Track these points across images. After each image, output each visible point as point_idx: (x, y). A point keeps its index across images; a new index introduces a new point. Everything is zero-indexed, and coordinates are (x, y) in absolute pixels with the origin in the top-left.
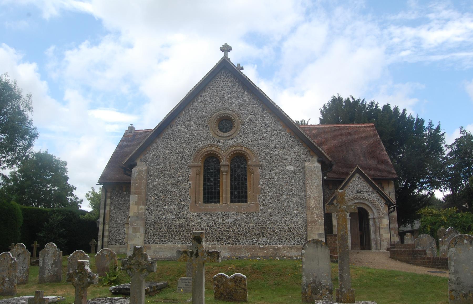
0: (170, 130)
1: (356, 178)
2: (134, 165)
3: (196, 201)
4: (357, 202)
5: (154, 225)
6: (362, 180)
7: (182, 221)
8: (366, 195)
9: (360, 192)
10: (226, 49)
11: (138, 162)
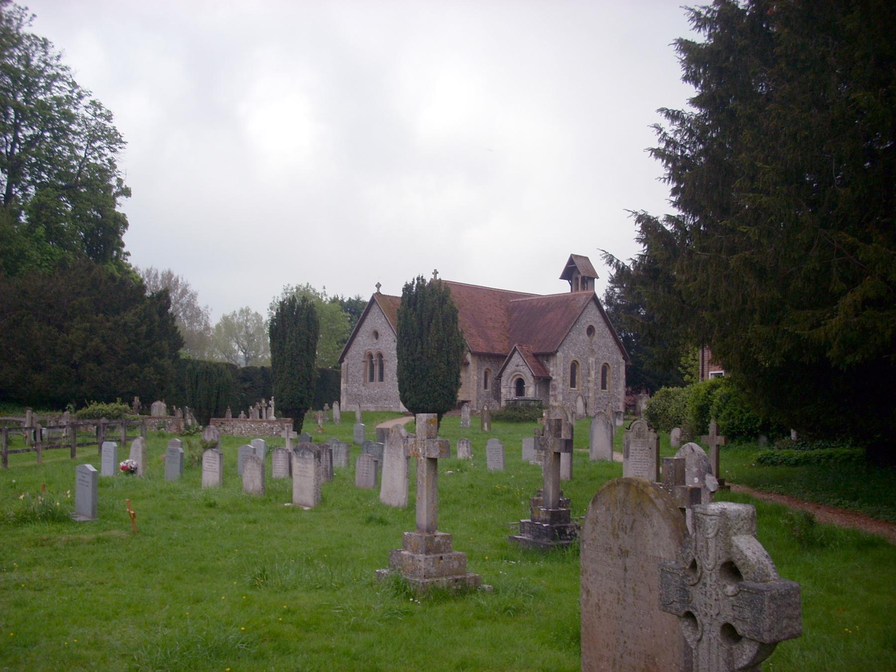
0: (356, 340)
1: (516, 354)
2: (343, 361)
3: (365, 381)
4: (516, 373)
5: (350, 395)
6: (519, 356)
7: (359, 393)
8: (521, 368)
9: (517, 366)
10: (378, 286)
11: (345, 359)
